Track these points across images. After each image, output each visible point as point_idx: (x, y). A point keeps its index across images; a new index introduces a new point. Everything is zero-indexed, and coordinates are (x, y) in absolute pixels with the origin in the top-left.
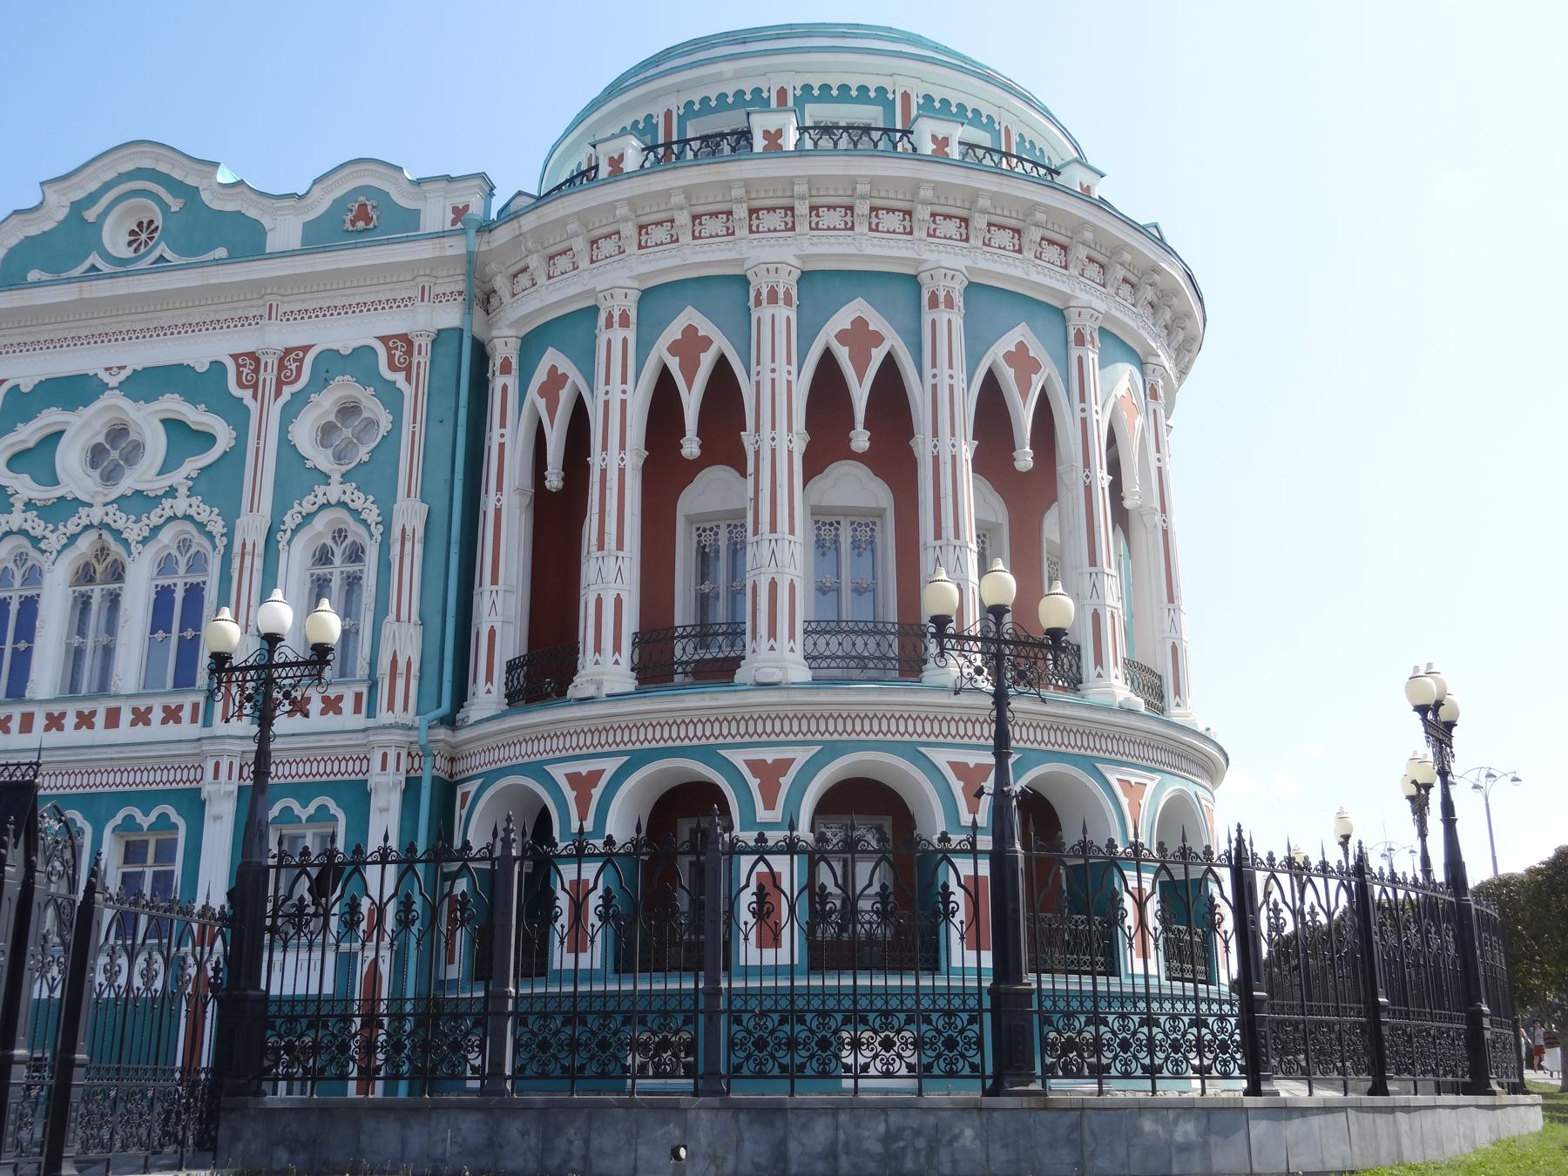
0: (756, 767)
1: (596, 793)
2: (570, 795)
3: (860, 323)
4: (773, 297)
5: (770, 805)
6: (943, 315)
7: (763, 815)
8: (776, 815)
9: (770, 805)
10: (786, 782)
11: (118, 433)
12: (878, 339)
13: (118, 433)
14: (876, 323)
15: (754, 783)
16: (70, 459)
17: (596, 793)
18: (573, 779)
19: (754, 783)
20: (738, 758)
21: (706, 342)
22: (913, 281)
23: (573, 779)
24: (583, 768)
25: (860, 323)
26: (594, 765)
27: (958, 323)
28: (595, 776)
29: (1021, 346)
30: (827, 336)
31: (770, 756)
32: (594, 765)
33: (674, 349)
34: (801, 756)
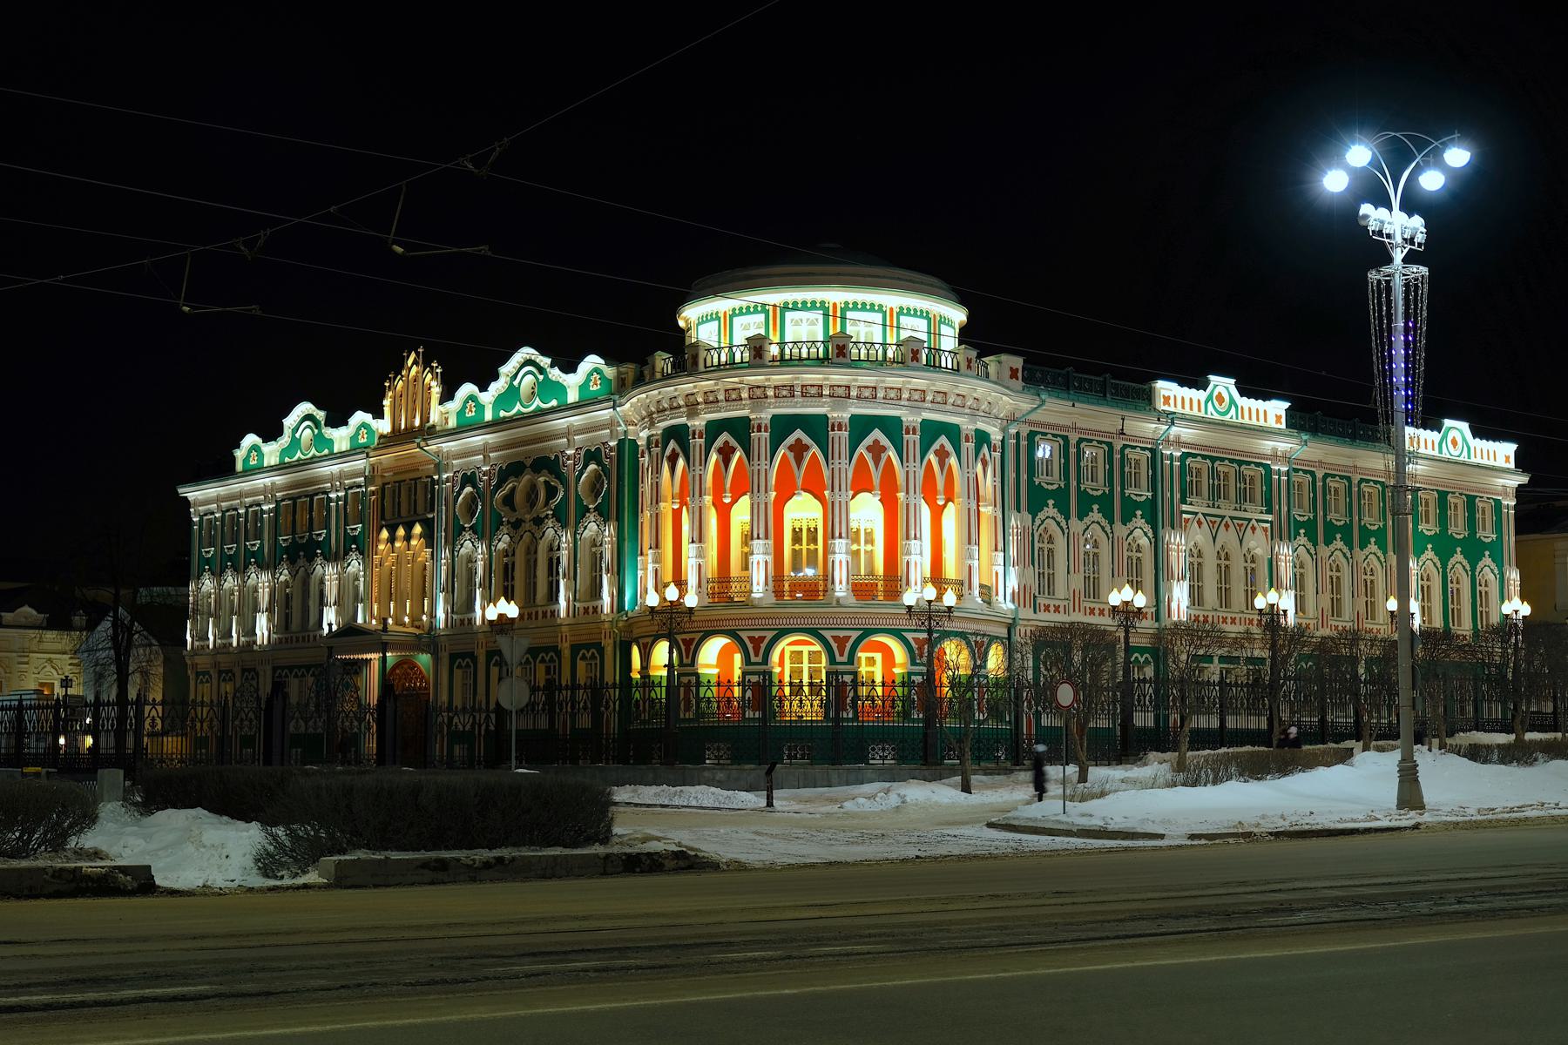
1: (763, 646)
2: (750, 646)
3: (876, 442)
5: (842, 655)
6: (910, 437)
7: (839, 659)
9: (842, 655)
10: (849, 645)
12: (884, 449)
15: (834, 646)
17: (763, 646)
20: (827, 634)
21: (807, 448)
24: (757, 634)
25: (876, 442)
30: (861, 449)
33: (791, 448)
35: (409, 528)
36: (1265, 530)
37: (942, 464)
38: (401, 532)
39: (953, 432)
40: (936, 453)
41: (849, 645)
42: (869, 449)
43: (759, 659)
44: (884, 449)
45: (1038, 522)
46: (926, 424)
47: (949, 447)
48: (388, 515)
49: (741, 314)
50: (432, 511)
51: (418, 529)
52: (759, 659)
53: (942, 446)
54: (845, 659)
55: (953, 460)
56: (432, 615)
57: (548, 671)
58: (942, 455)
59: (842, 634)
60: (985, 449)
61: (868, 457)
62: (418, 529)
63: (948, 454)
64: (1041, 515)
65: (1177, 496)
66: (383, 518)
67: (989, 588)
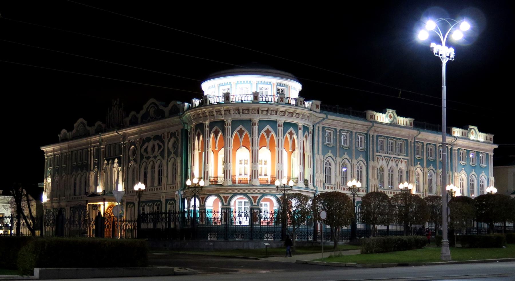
0: (253, 197)
1: (228, 199)
3: (268, 129)
4: (255, 125)
5: (255, 203)
6: (280, 128)
7: (254, 204)
9: (255, 203)
10: (257, 199)
12: (270, 132)
14: (271, 129)
15: (252, 199)
17: (228, 199)
18: (224, 197)
19: (252, 199)
20: (250, 196)
22: (276, 122)
23: (224, 197)
24: (226, 195)
25: (268, 129)
26: (227, 195)
27: (282, 128)
28: (228, 197)
29: (291, 131)
30: (263, 132)
32: (227, 195)
36: (406, 162)
37: (291, 137)
39: (295, 126)
40: (289, 133)
41: (257, 199)
42: (265, 132)
43: (227, 204)
44: (270, 132)
45: (325, 158)
46: (285, 123)
49: (222, 85)
52: (227, 204)
53: (291, 131)
54: (256, 204)
55: (295, 136)
58: (291, 134)
59: (255, 195)
60: (307, 133)
61: (265, 134)
63: (293, 134)
64: (326, 156)
65: (375, 149)
67: (307, 181)
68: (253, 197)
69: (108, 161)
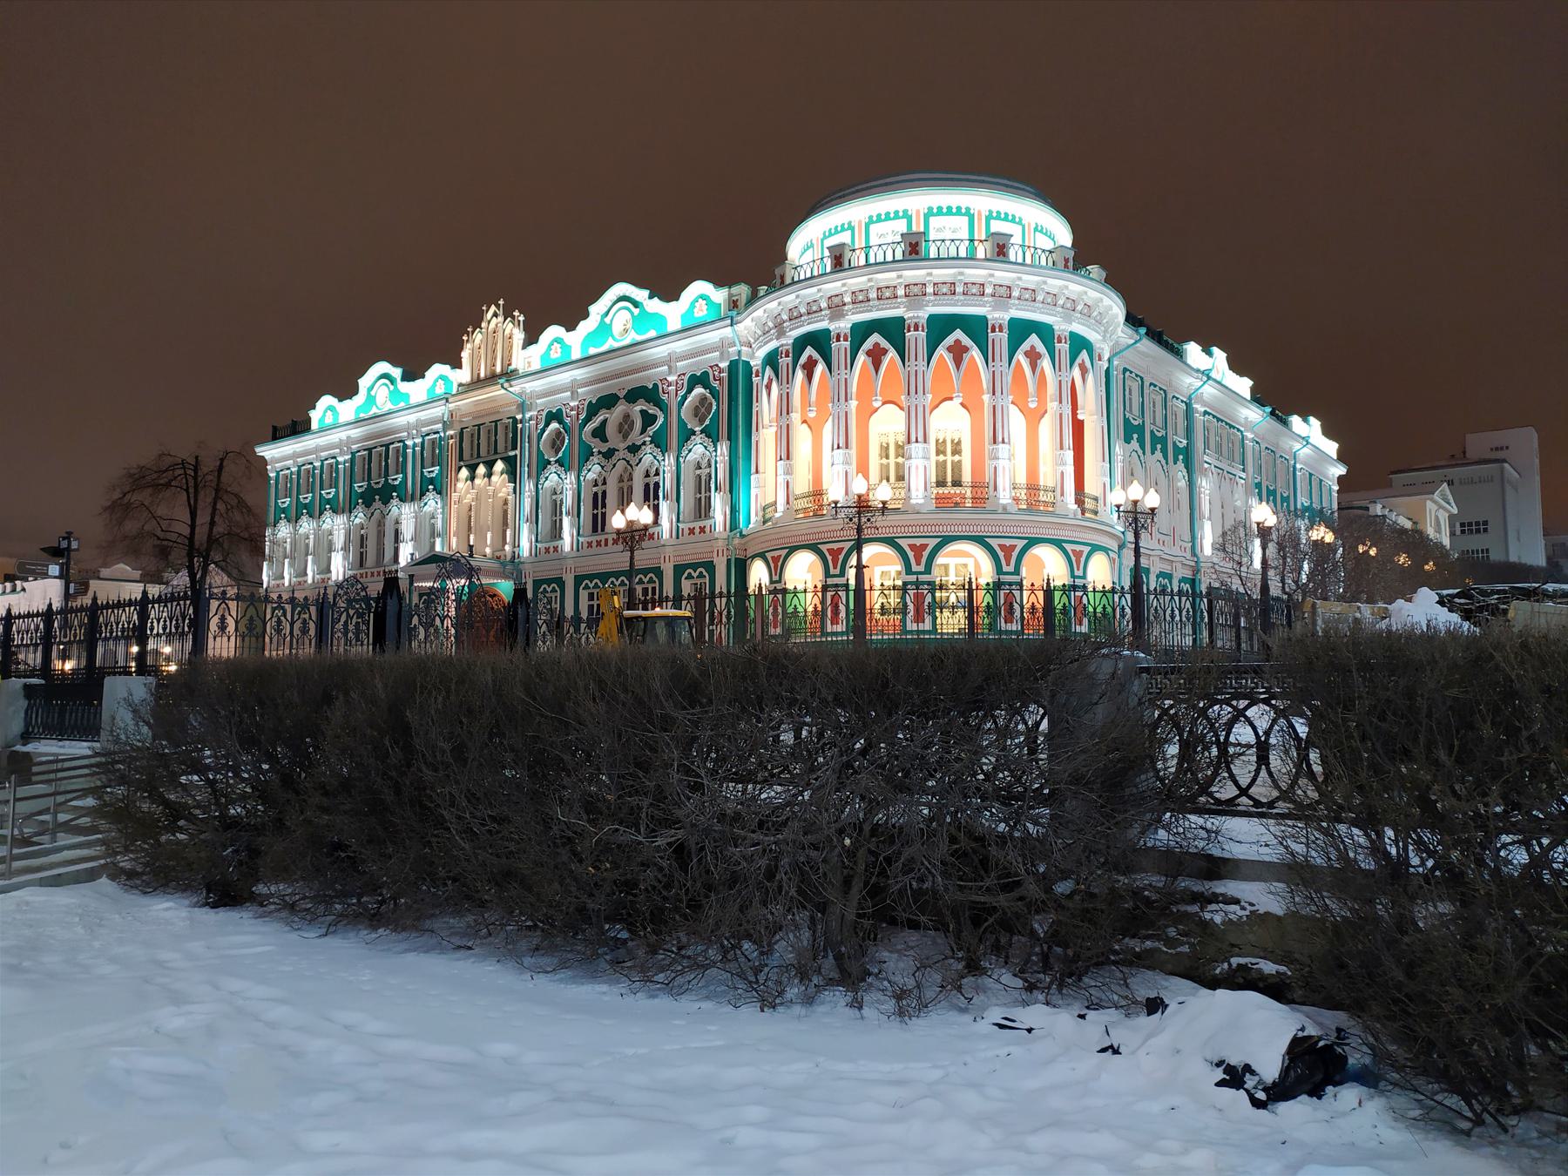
0: (912, 547)
3: (957, 342)
5: (918, 563)
7: (915, 568)
8: (921, 568)
9: (918, 563)
10: (926, 554)
11: (627, 417)
12: (966, 349)
13: (627, 417)
16: (611, 430)
19: (911, 554)
25: (957, 342)
31: (918, 542)
34: (932, 543)
35: (490, 465)
37: (1034, 367)
38: (481, 470)
40: (1027, 354)
41: (926, 554)
42: (949, 349)
44: (966, 349)
47: (1041, 348)
48: (466, 455)
50: (514, 448)
51: (499, 466)
55: (1046, 363)
56: (516, 544)
57: (591, 597)
58: (1033, 356)
60: (1084, 355)
61: (948, 358)
62: (499, 466)
63: (1039, 356)
66: (461, 459)
68: (912, 547)
69: (472, 468)
